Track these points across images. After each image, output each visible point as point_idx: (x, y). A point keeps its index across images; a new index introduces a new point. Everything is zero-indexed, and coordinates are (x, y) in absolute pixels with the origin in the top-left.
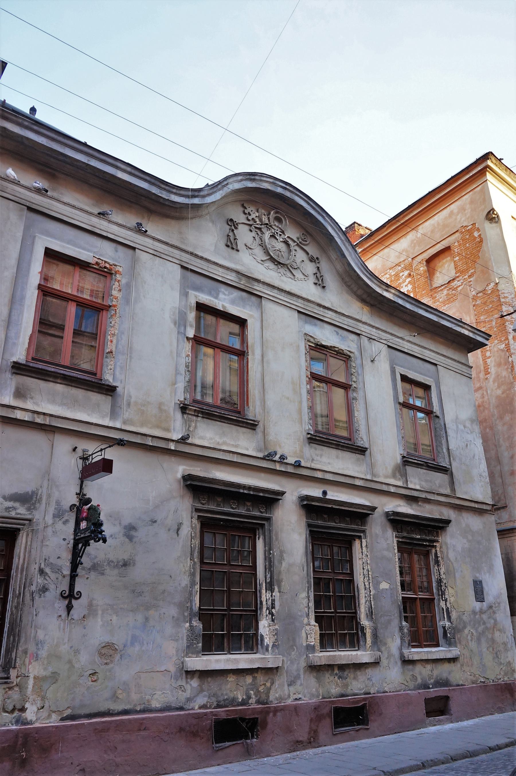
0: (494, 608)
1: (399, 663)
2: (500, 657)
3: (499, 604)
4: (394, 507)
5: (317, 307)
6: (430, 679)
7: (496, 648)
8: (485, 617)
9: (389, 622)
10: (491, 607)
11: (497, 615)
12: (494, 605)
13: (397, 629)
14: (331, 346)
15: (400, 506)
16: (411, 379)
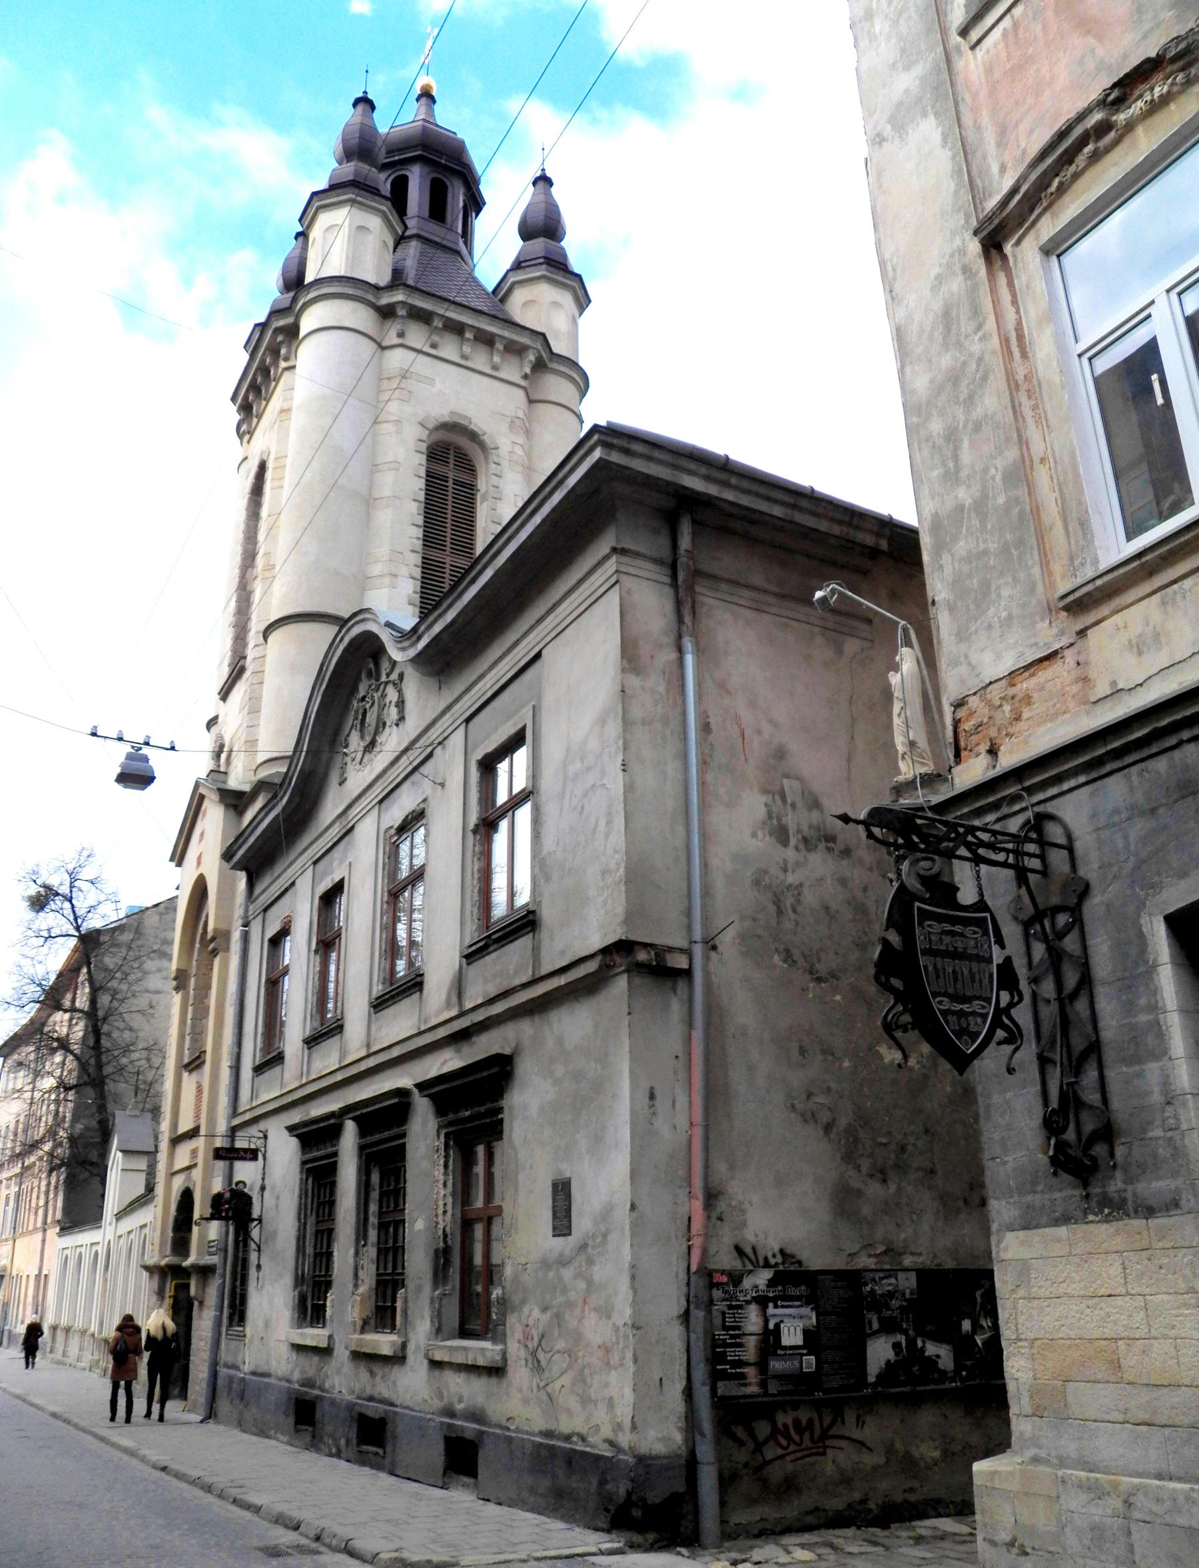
0: (590, 1250)
1: (426, 1362)
2: (588, 1381)
3: (605, 1236)
4: (440, 1068)
5: (392, 770)
6: (460, 1401)
7: (584, 1357)
8: (567, 1273)
9: (419, 1288)
10: (583, 1247)
11: (596, 1268)
12: (591, 1243)
13: (427, 1302)
14: (404, 820)
15: (446, 1061)
16: (496, 750)
